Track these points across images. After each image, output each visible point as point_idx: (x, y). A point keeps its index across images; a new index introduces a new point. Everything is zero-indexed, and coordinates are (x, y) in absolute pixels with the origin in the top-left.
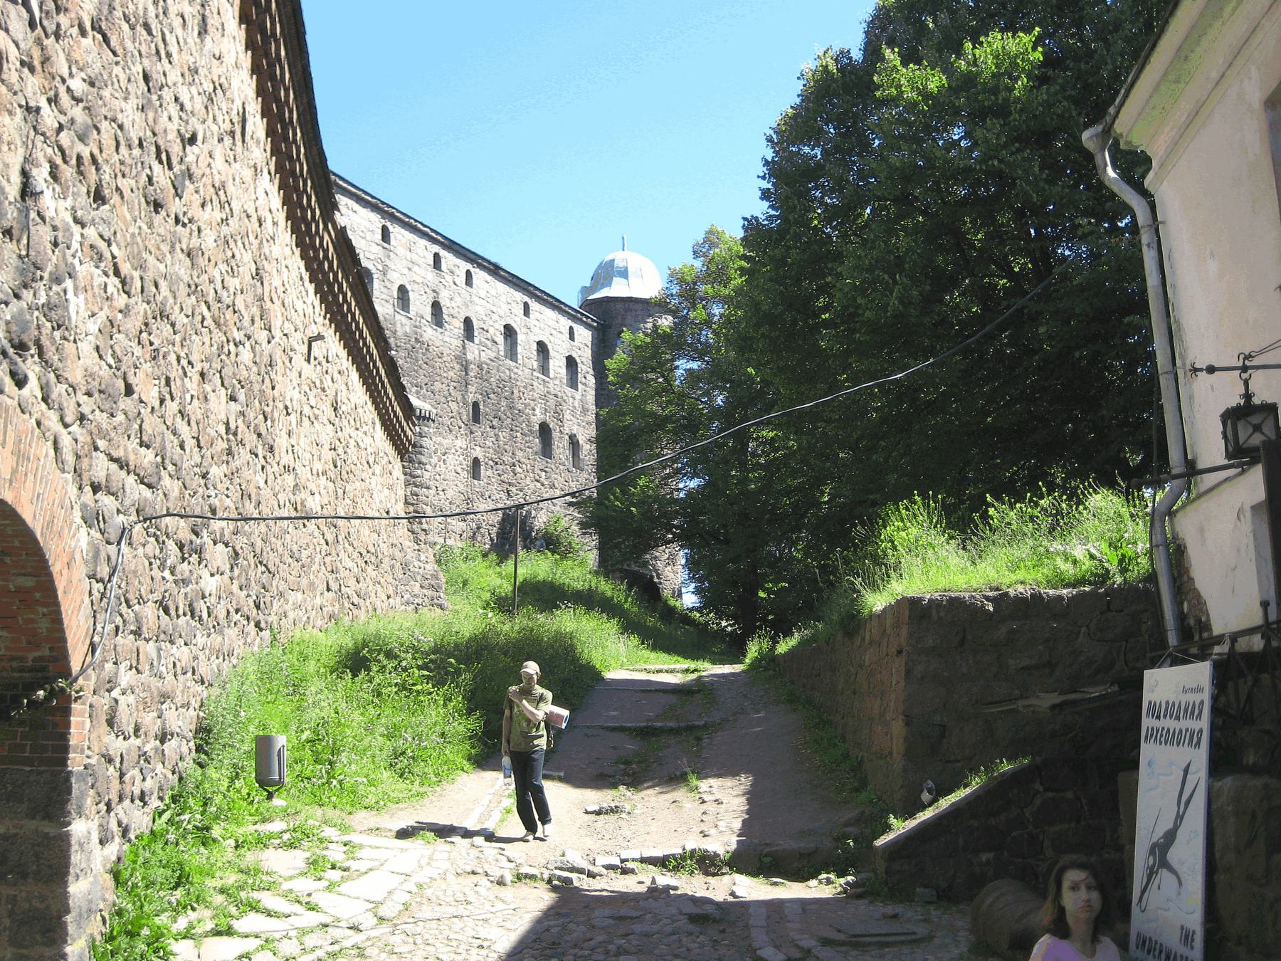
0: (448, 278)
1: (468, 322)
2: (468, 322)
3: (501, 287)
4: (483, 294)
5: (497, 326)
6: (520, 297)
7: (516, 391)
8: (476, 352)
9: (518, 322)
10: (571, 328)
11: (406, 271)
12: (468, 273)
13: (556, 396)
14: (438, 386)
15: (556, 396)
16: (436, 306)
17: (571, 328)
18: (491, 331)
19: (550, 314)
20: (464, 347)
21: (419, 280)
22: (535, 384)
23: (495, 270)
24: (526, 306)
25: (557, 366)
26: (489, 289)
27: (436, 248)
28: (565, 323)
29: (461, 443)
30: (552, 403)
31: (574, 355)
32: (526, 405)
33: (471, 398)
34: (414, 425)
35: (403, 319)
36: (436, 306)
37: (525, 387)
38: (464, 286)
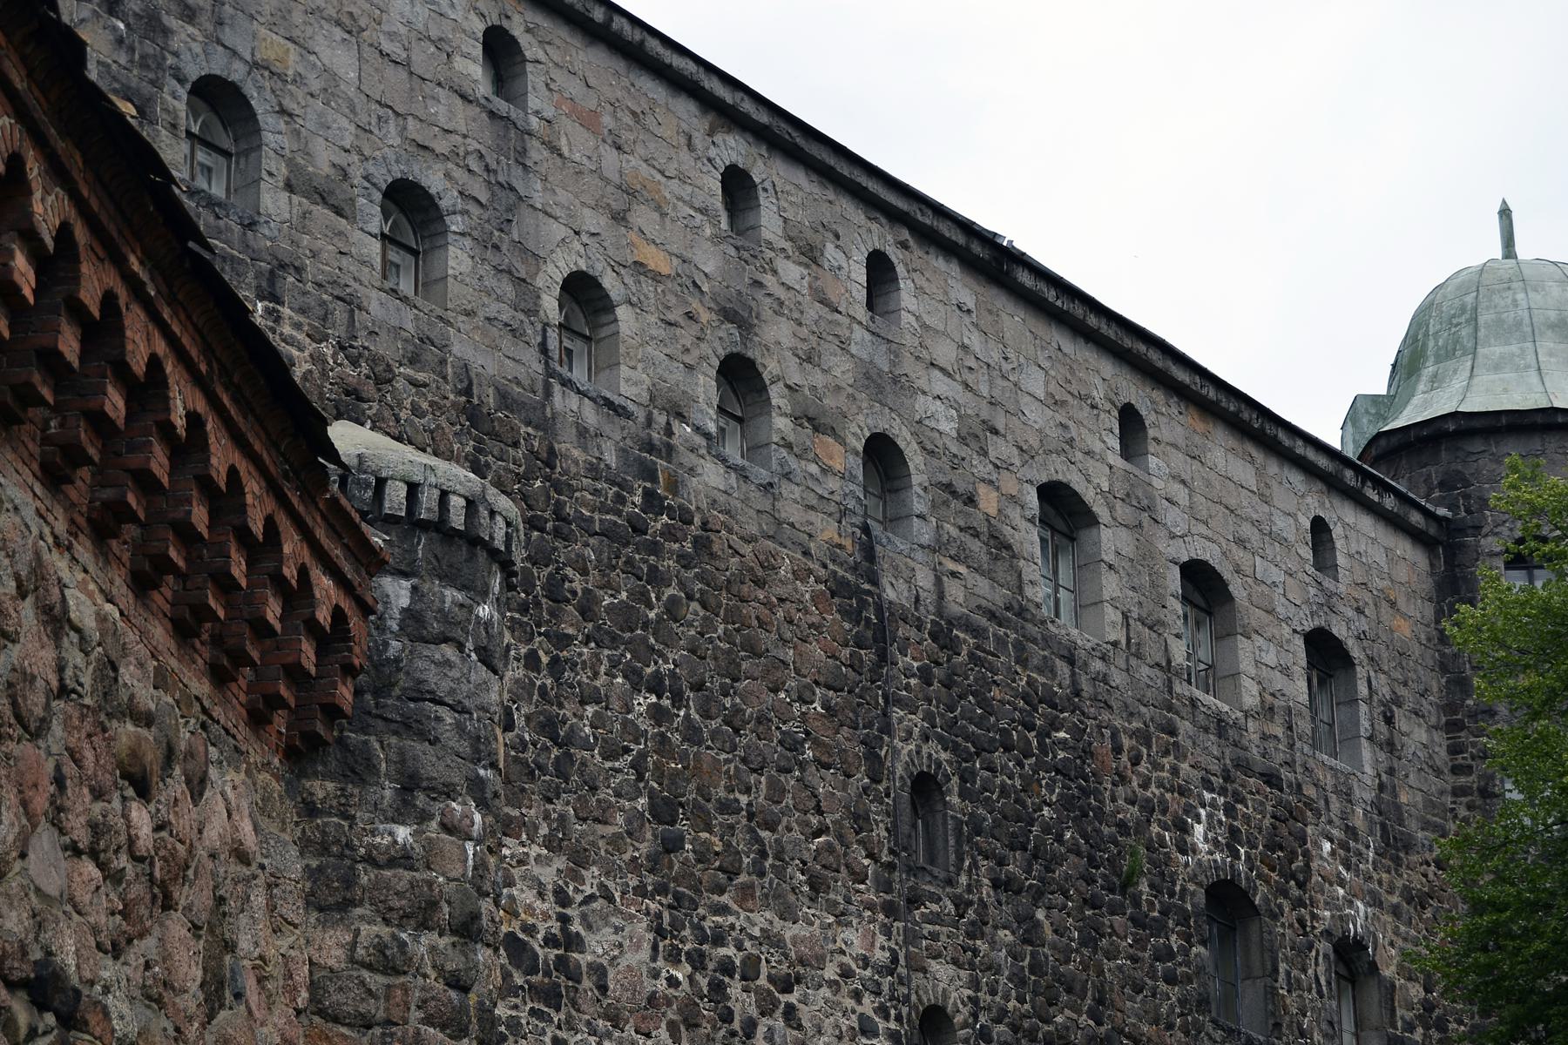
0: (792, 272)
1: (881, 455)
2: (881, 455)
3: (1015, 321)
4: (945, 353)
5: (1009, 484)
6: (1105, 379)
7: (1104, 747)
8: (924, 579)
9: (1096, 475)
10: (1319, 527)
11: (593, 221)
12: (879, 268)
13: (1271, 779)
14: (753, 697)
15: (1271, 779)
16: (740, 376)
17: (1319, 527)
18: (988, 501)
19: (1228, 459)
20: (869, 553)
21: (658, 261)
22: (1184, 727)
23: (993, 262)
24: (1130, 421)
25: (1268, 664)
26: (974, 340)
27: (733, 148)
28: (1296, 502)
29: (858, 939)
30: (1257, 810)
31: (1339, 630)
32: (1148, 808)
33: (907, 750)
34: (373, 563)
35: (591, 415)
36: (740, 376)
37: (1144, 737)
38: (861, 313)
